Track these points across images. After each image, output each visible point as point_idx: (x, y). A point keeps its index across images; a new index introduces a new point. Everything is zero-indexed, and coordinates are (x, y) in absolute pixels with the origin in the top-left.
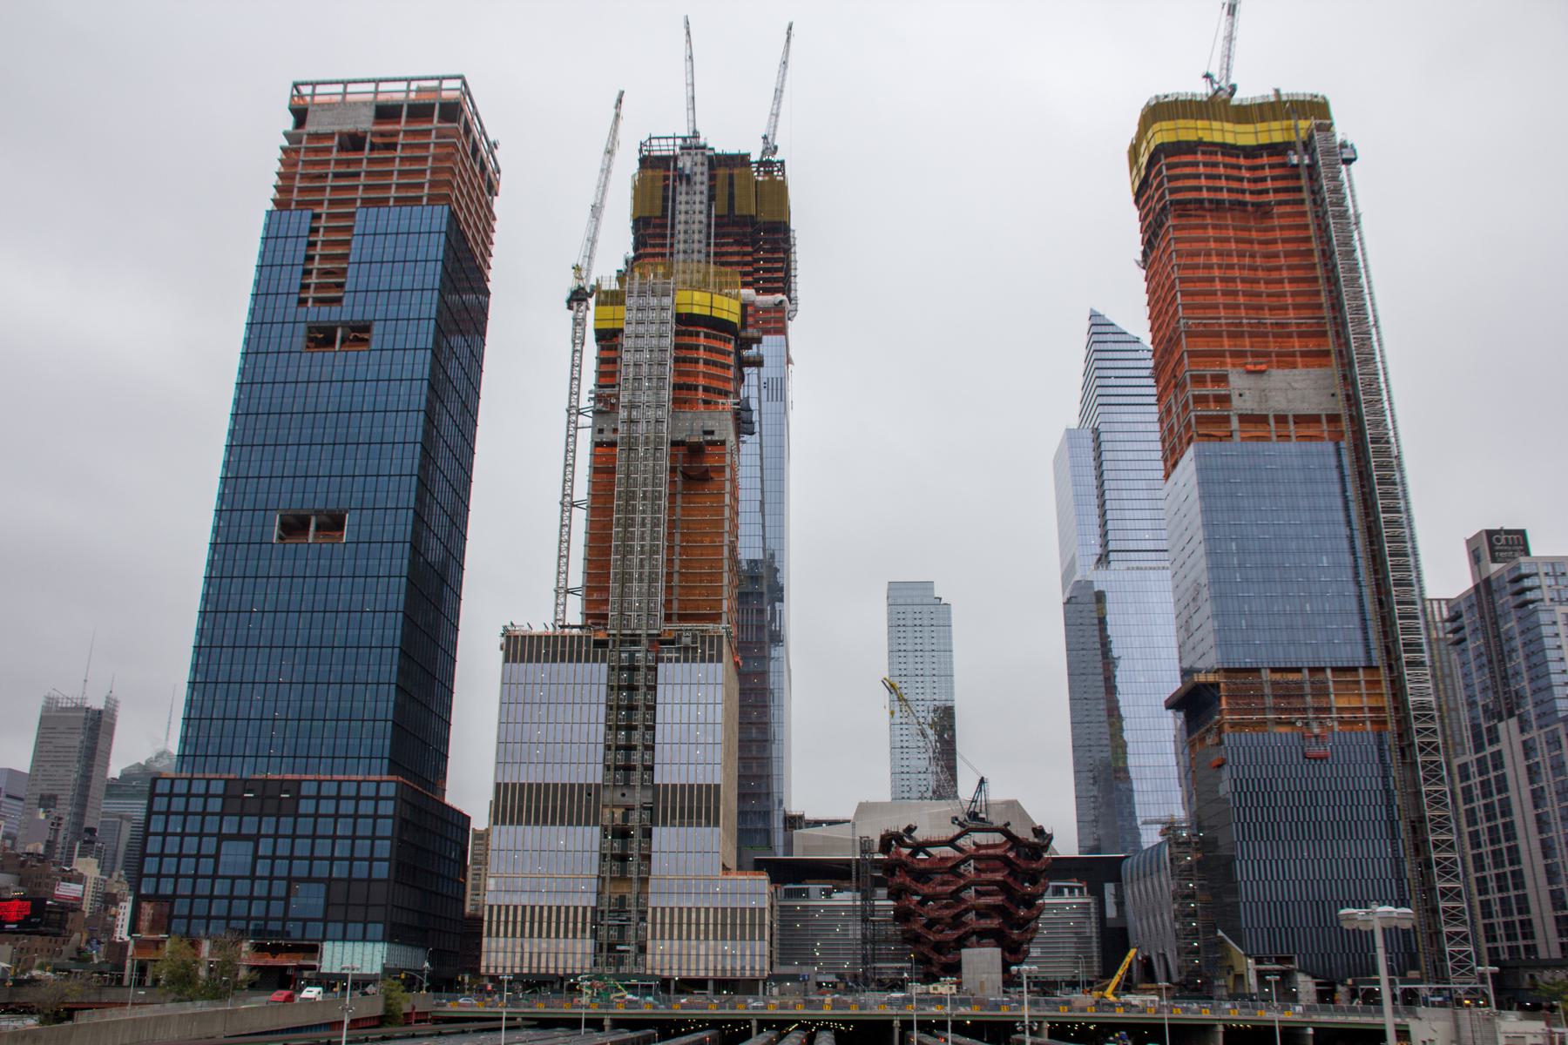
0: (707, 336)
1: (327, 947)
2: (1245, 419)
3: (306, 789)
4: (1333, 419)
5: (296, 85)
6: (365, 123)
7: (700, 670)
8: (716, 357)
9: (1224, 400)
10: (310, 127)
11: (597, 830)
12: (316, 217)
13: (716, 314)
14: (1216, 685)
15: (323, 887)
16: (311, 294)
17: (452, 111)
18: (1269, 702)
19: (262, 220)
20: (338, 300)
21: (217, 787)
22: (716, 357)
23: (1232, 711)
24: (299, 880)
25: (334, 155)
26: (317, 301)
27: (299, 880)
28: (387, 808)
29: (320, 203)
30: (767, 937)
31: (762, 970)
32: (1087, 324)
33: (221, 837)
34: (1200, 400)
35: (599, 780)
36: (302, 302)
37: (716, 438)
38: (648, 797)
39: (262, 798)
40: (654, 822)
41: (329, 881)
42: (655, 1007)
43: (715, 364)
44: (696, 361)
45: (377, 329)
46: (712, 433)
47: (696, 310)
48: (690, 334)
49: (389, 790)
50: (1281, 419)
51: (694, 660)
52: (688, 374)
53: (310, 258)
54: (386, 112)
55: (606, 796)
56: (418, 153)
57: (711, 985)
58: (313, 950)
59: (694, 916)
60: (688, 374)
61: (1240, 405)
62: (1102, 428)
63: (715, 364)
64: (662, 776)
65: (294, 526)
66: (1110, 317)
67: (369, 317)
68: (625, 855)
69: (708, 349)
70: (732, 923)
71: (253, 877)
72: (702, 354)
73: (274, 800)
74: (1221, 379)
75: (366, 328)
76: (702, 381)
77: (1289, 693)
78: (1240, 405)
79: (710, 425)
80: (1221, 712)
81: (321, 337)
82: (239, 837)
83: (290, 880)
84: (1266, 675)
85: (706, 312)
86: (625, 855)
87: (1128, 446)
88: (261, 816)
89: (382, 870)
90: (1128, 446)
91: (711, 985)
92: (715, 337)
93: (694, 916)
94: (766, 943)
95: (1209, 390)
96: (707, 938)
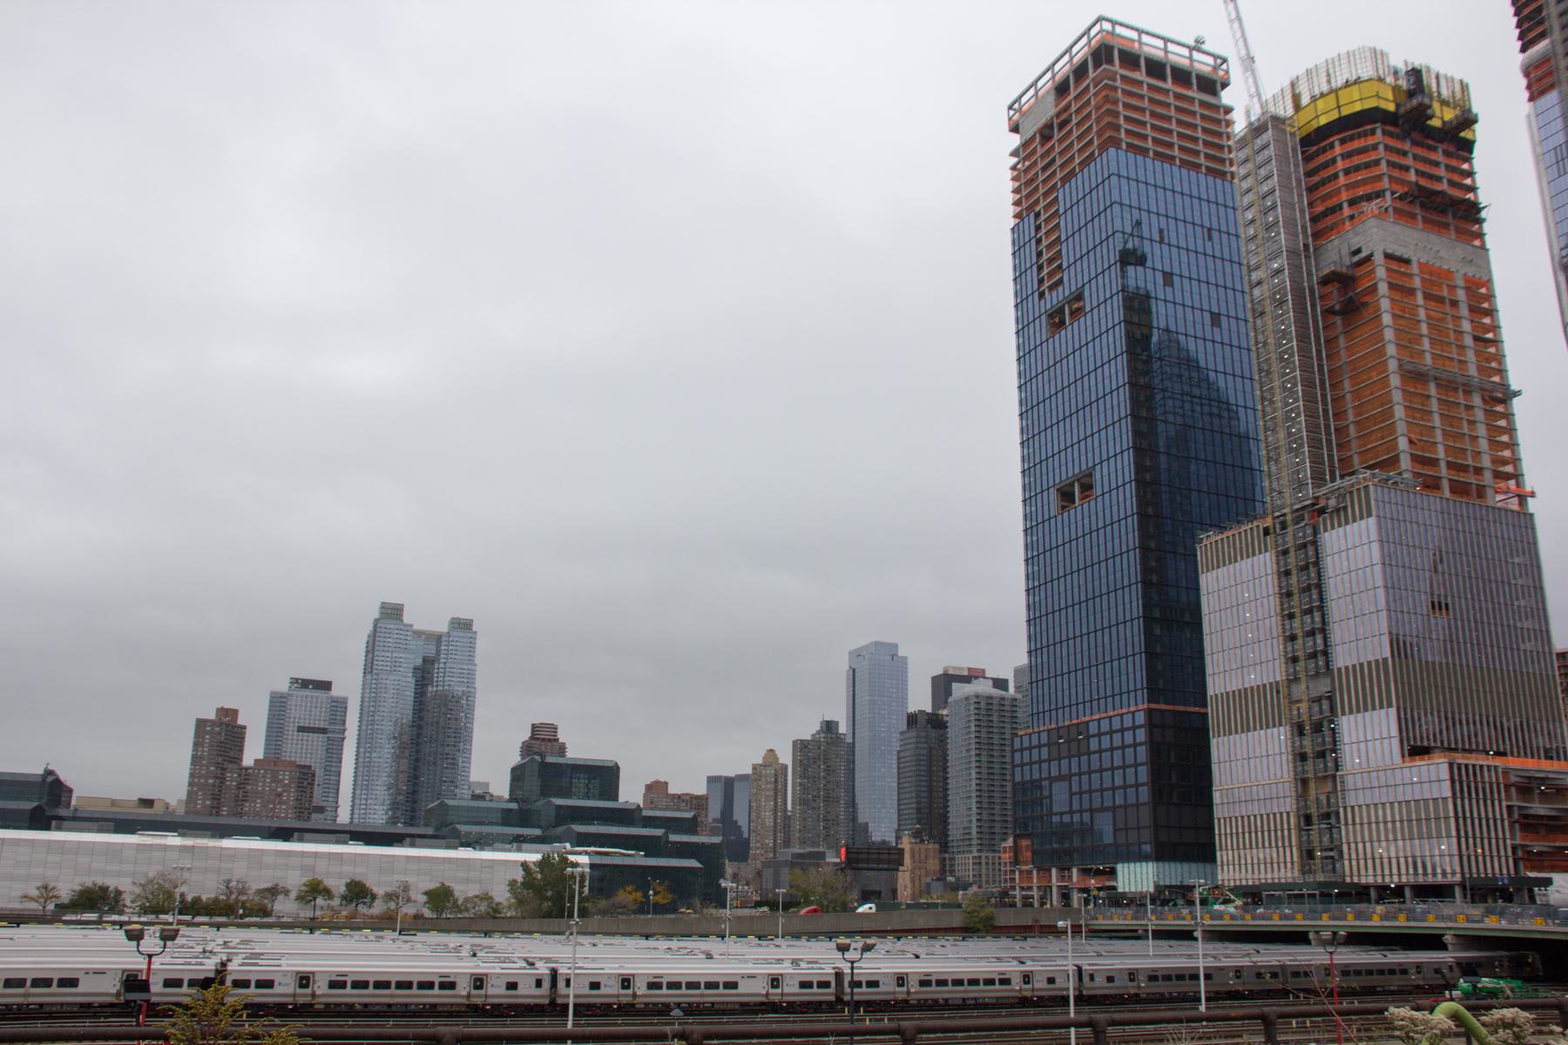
0: (1343, 142)
1: (1121, 868)
3: (1093, 729)
5: (1010, 108)
6: (1049, 110)
7: (1353, 529)
8: (1357, 160)
12: (1037, 215)
13: (1346, 111)
15: (1110, 814)
16: (1047, 284)
17: (1102, 54)
19: (1007, 238)
20: (1060, 282)
21: (1044, 739)
22: (1357, 160)
24: (1096, 810)
25: (1040, 151)
26: (1051, 288)
27: (1096, 810)
28: (1141, 735)
29: (1037, 202)
30: (1454, 833)
31: (1453, 873)
33: (1052, 780)
36: (1042, 295)
37: (1363, 255)
38: (1322, 687)
39: (1068, 742)
41: (1114, 808)
42: (1232, 917)
43: (1357, 169)
44: (1336, 176)
46: (1358, 251)
47: (1323, 121)
48: (1324, 150)
49: (1141, 718)
51: (1347, 523)
52: (1330, 196)
53: (1039, 254)
54: (1061, 89)
56: (1085, 112)
57: (1408, 893)
58: (1112, 873)
59: (1380, 813)
60: (1330, 196)
63: (1357, 169)
64: (1343, 658)
65: (1066, 496)
68: (1317, 753)
69: (1346, 156)
70: (1418, 817)
71: (1071, 812)
72: (1340, 164)
73: (1072, 741)
75: (1079, 297)
76: (1345, 196)
79: (1356, 242)
81: (1057, 321)
82: (1060, 778)
83: (1092, 811)
85: (1334, 116)
86: (1317, 753)
88: (1070, 758)
89: (1145, 794)
91: (1458, 891)
92: (1352, 138)
93: (1380, 813)
94: (1454, 840)
96: (1395, 840)
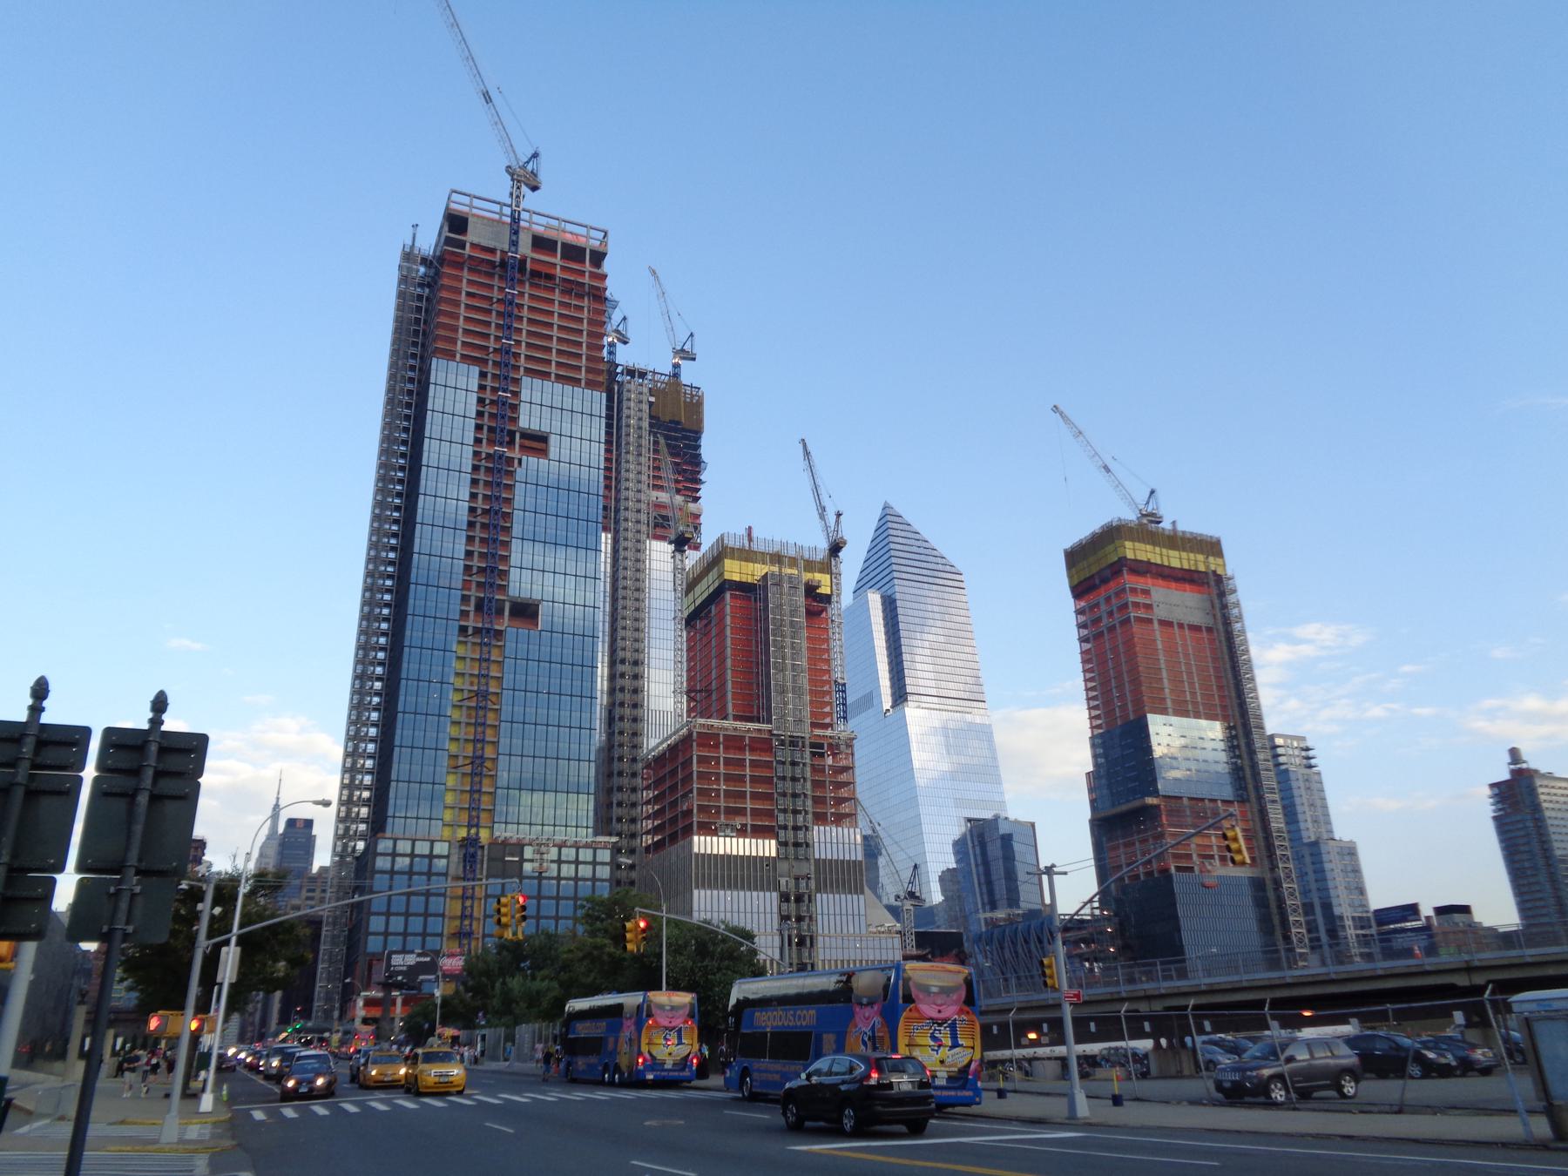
2: (1163, 623)
4: (1209, 630)
9: (1149, 607)
10: (472, 237)
11: (775, 894)
14: (1157, 807)
18: (1189, 820)
23: (1171, 825)
32: (878, 513)
34: (1136, 605)
35: (774, 854)
40: (818, 890)
45: (553, 440)
50: (1181, 626)
55: (783, 867)
61: (1160, 612)
62: (898, 596)
66: (899, 509)
67: (545, 428)
74: (1146, 592)
77: (1199, 815)
78: (1160, 612)
80: (1162, 826)
84: (1185, 801)
87: (916, 613)
90: (916, 613)
95: (1140, 599)
